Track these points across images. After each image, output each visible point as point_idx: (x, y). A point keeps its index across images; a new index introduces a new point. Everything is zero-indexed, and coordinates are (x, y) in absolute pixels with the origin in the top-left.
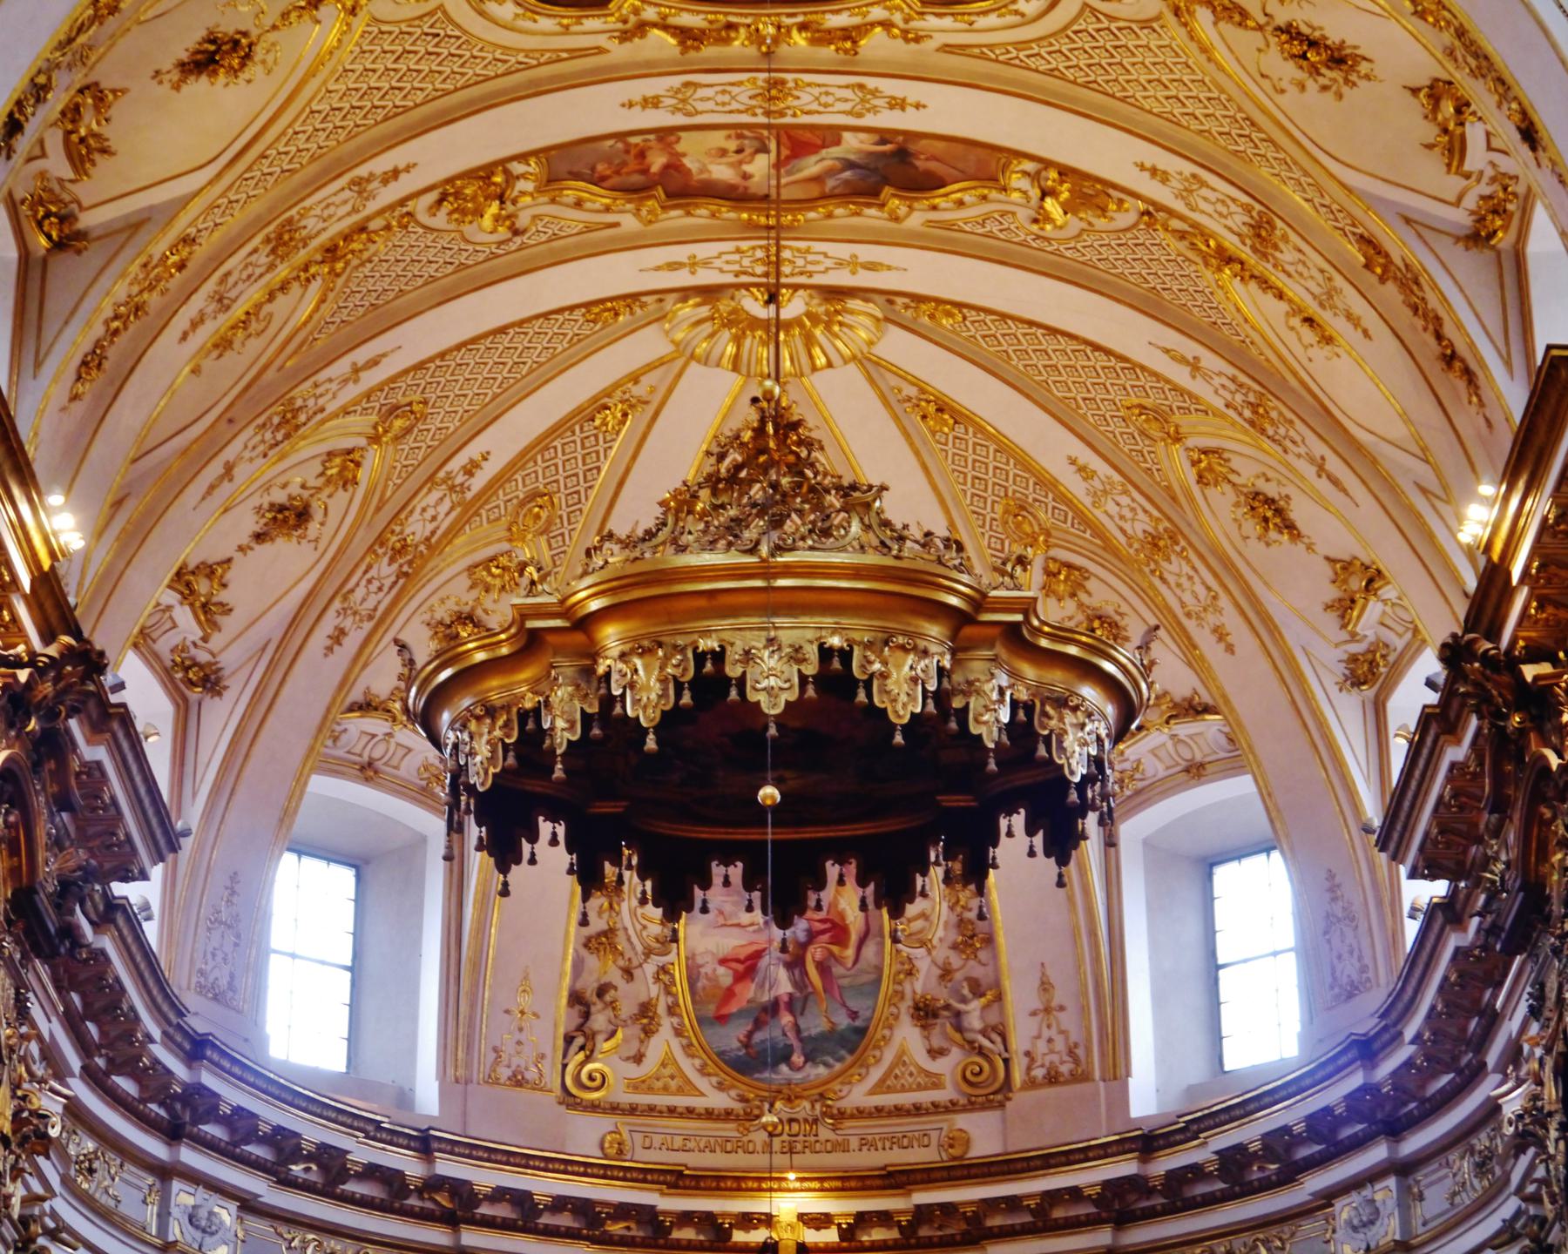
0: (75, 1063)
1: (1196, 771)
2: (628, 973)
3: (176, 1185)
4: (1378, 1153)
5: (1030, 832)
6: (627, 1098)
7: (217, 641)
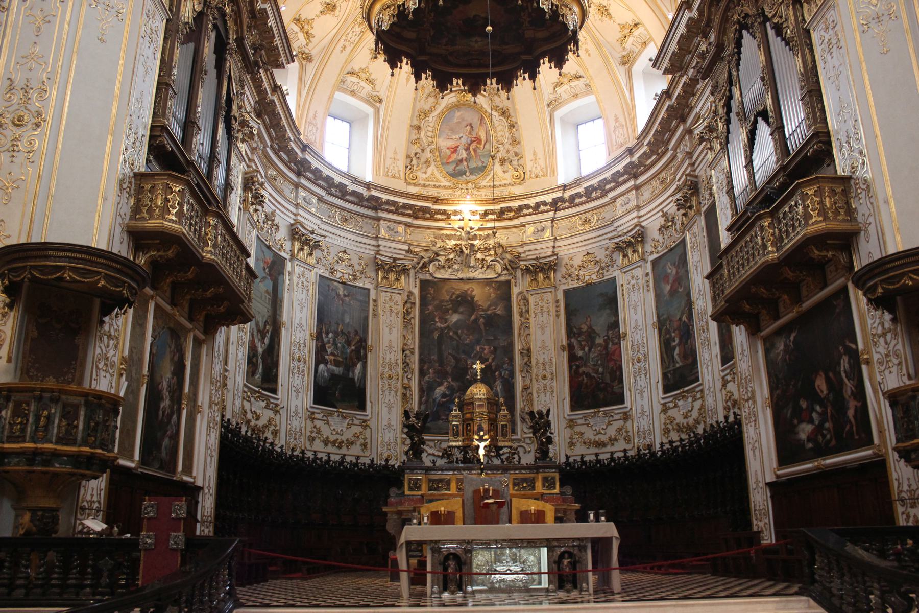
0: (269, 144)
1: (576, 96)
2: (423, 150)
3: (300, 189)
4: (631, 183)
5: (550, 62)
6: (422, 182)
7: (311, 46)
